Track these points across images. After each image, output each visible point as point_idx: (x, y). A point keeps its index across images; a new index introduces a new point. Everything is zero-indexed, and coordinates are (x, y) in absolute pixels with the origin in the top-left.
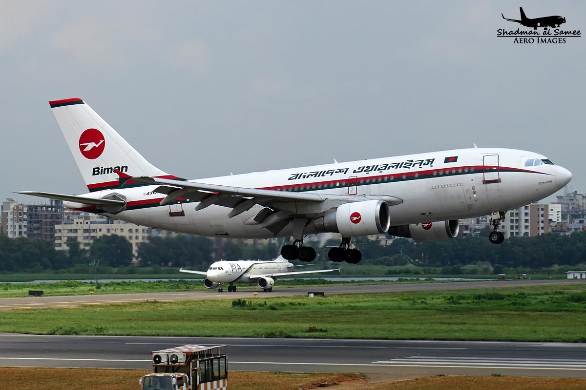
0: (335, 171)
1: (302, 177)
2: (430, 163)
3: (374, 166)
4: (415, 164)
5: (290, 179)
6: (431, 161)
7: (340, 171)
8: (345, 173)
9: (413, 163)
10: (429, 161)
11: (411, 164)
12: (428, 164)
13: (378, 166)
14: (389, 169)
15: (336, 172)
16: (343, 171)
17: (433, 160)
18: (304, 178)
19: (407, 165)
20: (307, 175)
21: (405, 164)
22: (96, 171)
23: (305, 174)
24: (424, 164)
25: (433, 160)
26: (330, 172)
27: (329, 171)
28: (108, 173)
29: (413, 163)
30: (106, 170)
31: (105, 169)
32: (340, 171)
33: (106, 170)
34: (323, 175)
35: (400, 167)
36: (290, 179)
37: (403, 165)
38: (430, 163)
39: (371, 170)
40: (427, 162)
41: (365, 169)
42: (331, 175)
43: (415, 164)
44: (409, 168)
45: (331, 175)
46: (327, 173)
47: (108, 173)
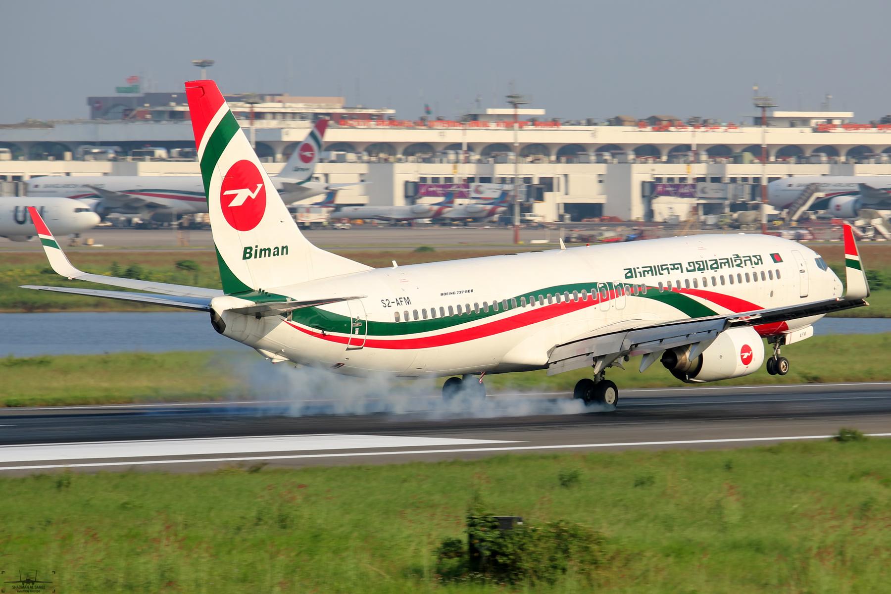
1: (638, 274)
2: (760, 261)
5: (627, 277)
8: (682, 272)
12: (757, 264)
14: (721, 268)
15: (672, 269)
16: (678, 268)
18: (641, 276)
19: (738, 262)
22: (248, 253)
24: (756, 264)
26: (664, 267)
27: (662, 266)
29: (743, 259)
30: (263, 252)
31: (261, 250)
32: (675, 267)
36: (627, 277)
37: (735, 264)
38: (760, 261)
39: (704, 269)
41: (697, 266)
42: (669, 273)
44: (742, 267)
45: (669, 273)
46: (663, 270)
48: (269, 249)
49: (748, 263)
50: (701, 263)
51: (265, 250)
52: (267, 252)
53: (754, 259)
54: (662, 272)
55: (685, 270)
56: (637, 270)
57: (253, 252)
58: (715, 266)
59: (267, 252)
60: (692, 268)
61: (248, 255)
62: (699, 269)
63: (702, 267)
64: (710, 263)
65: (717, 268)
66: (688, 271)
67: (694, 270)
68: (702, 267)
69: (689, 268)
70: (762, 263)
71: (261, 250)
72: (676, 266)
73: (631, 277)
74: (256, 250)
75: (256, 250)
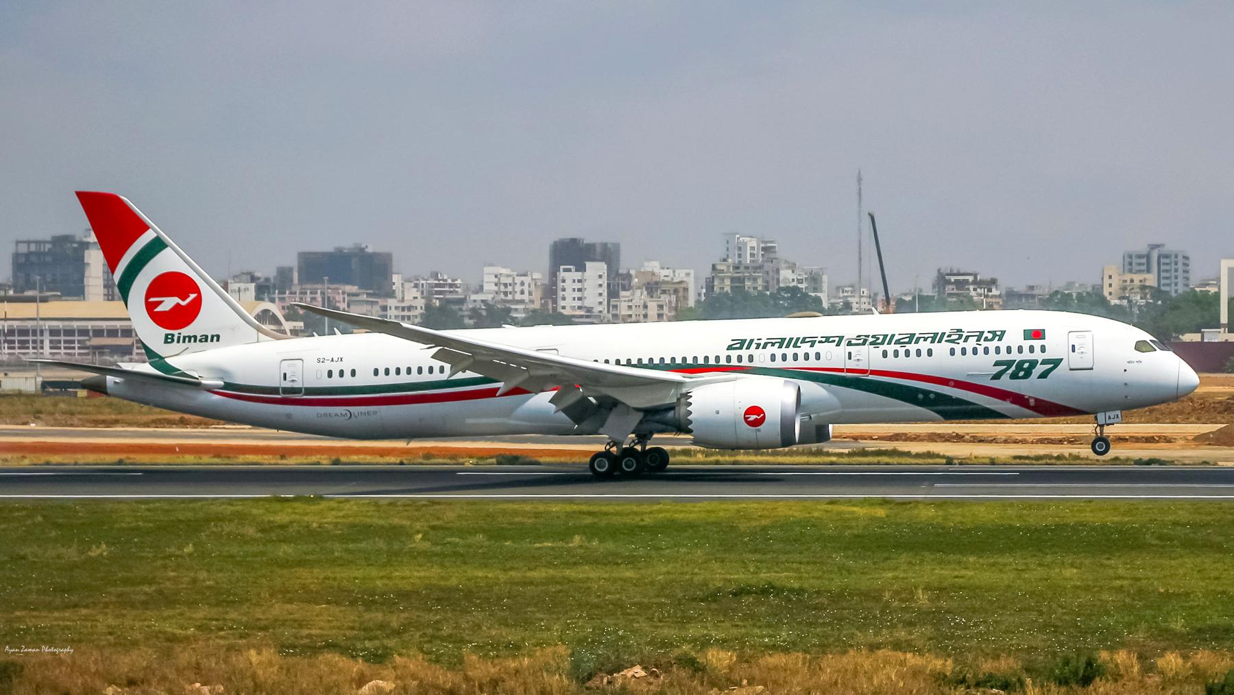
0: (819, 339)
1: (754, 346)
2: (997, 338)
3: (886, 336)
4: (967, 337)
6: (999, 333)
7: (828, 340)
9: (965, 335)
10: (994, 333)
11: (960, 338)
12: (992, 339)
13: (893, 336)
15: (819, 342)
16: (834, 341)
17: (1003, 332)
18: (758, 346)
20: (762, 343)
21: (949, 336)
22: (168, 340)
23: (759, 342)
24: (986, 339)
25: (1003, 332)
26: (807, 340)
27: (805, 338)
28: (190, 341)
29: (965, 335)
30: (187, 339)
31: (184, 337)
32: (828, 340)
33: (187, 339)
34: (795, 346)
35: (940, 342)
36: (730, 348)
37: (945, 338)
38: (997, 338)
39: (882, 343)
40: (990, 336)
41: (871, 339)
42: (812, 346)
43: (967, 337)
45: (812, 346)
46: (804, 341)
47: (190, 341)
48: (195, 337)
49: (972, 341)
50: (881, 337)
51: (190, 338)
52: (193, 339)
53: (986, 334)
54: (799, 344)
55: (844, 343)
56: (755, 341)
57: (176, 338)
58: (907, 340)
59: (193, 339)
60: (861, 342)
61: (169, 340)
62: (871, 344)
63: (879, 341)
64: (897, 337)
65: (909, 342)
66: (849, 344)
67: (864, 344)
68: (879, 341)
69: (853, 342)
70: (1000, 340)
71: (184, 337)
72: (831, 339)
73: (741, 348)
74: (179, 338)
75: (179, 338)
